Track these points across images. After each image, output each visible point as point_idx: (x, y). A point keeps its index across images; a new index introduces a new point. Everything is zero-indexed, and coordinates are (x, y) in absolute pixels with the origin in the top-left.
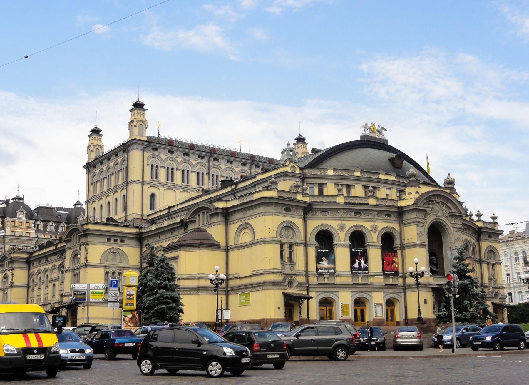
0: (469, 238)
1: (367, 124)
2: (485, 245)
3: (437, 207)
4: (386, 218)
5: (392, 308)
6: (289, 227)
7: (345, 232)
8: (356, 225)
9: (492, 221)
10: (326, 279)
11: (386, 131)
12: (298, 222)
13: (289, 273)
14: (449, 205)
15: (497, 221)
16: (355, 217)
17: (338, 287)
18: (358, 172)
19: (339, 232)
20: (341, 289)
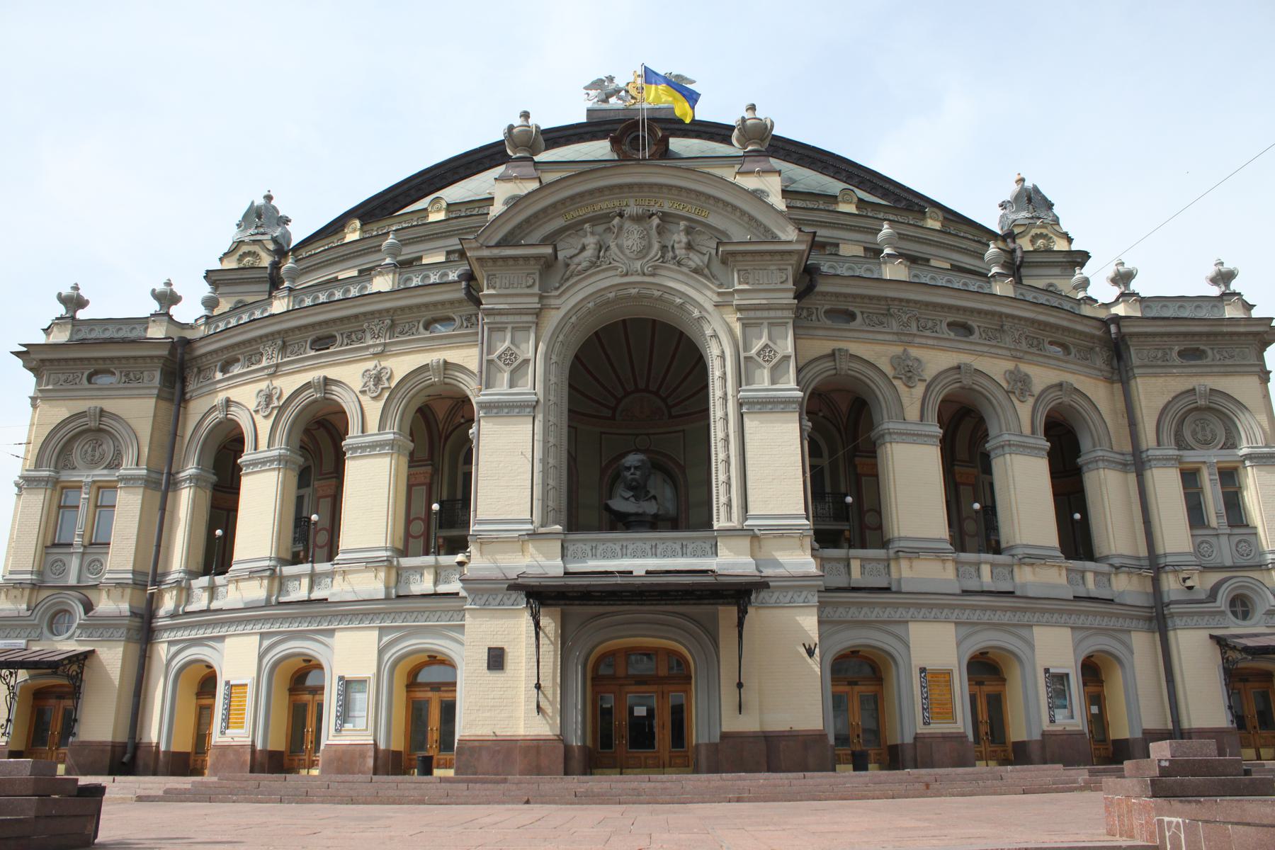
0: (996, 367)
1: (611, 79)
2: (1154, 392)
3: (632, 238)
4: (427, 334)
5: (447, 696)
6: (100, 430)
7: (275, 412)
8: (307, 386)
9: (1215, 291)
10: (206, 595)
11: (692, 82)
12: (138, 411)
13: (72, 581)
14: (714, 220)
15: (1235, 286)
16: (313, 353)
17: (222, 623)
18: (439, 210)
19: (258, 418)
20: (232, 630)
